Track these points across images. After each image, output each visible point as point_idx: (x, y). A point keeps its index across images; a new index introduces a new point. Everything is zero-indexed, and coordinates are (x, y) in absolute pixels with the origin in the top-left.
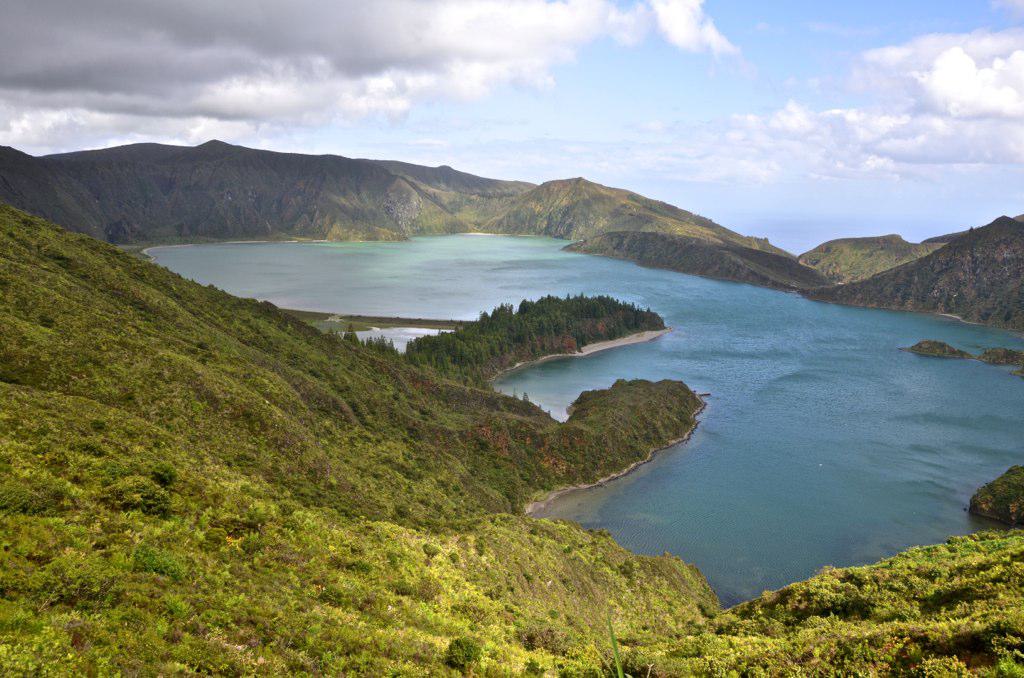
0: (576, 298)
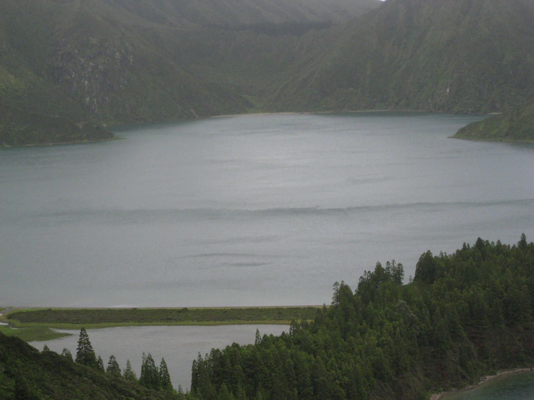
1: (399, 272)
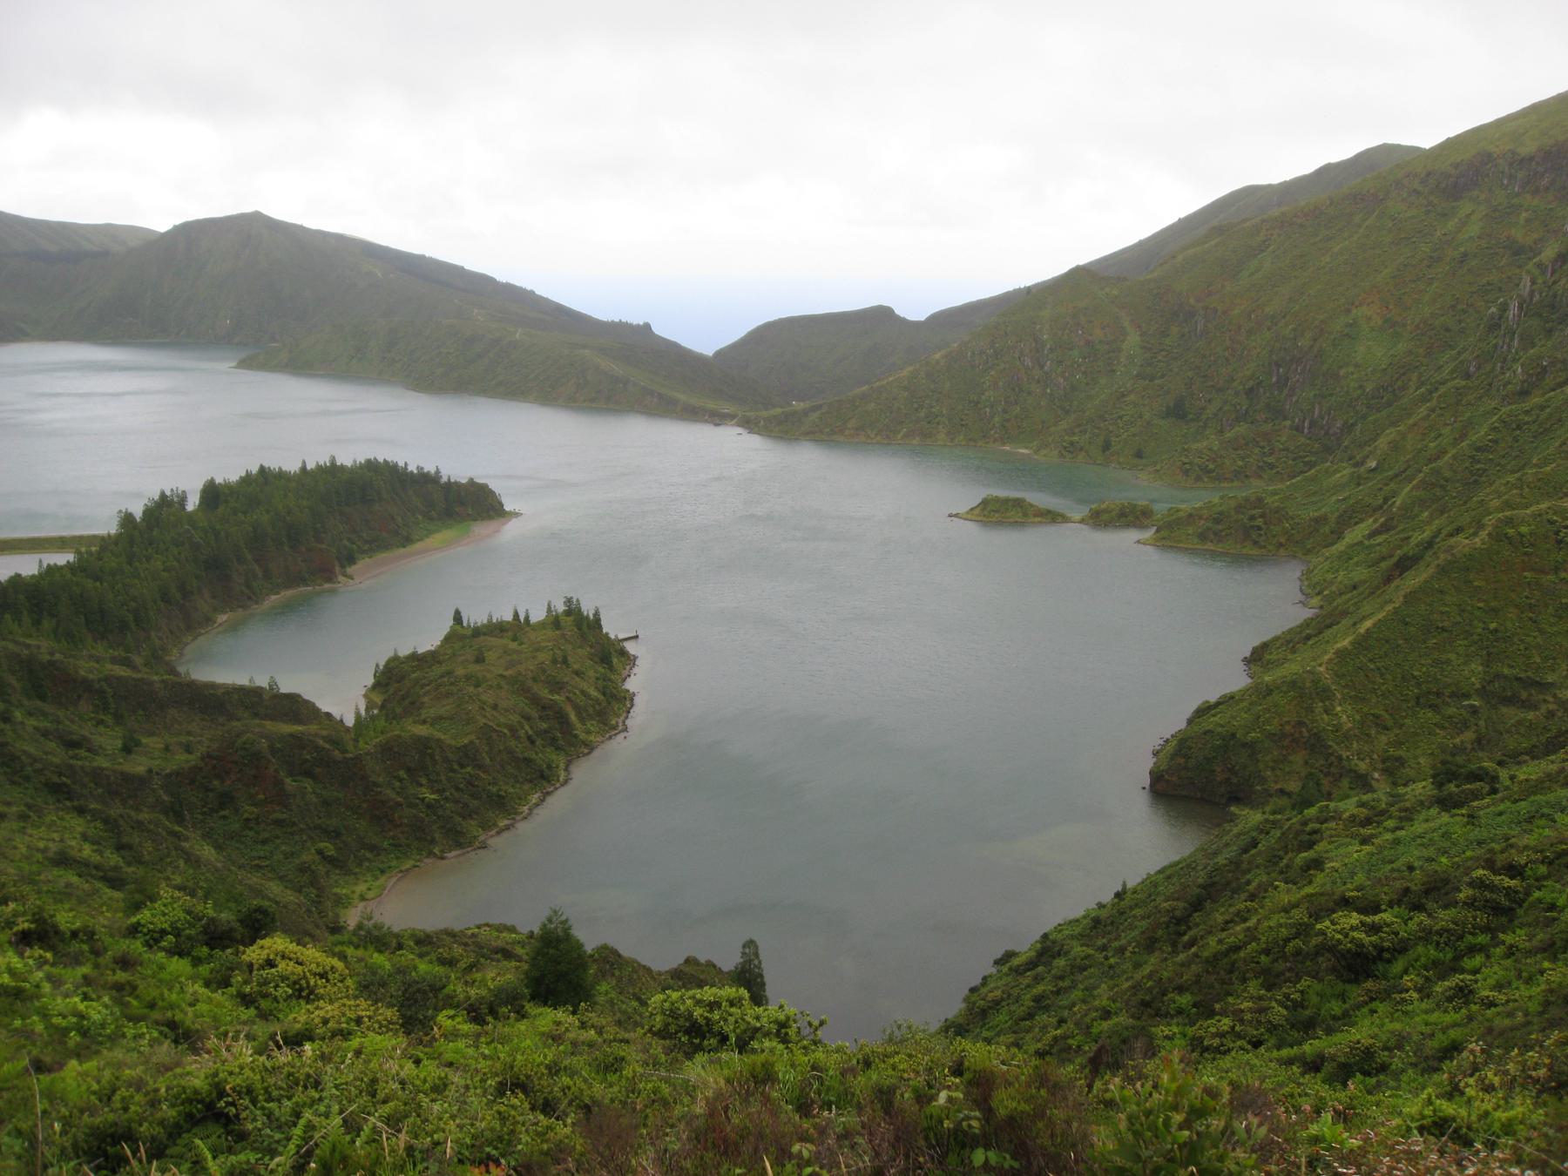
0: (319, 468)
1: (183, 499)
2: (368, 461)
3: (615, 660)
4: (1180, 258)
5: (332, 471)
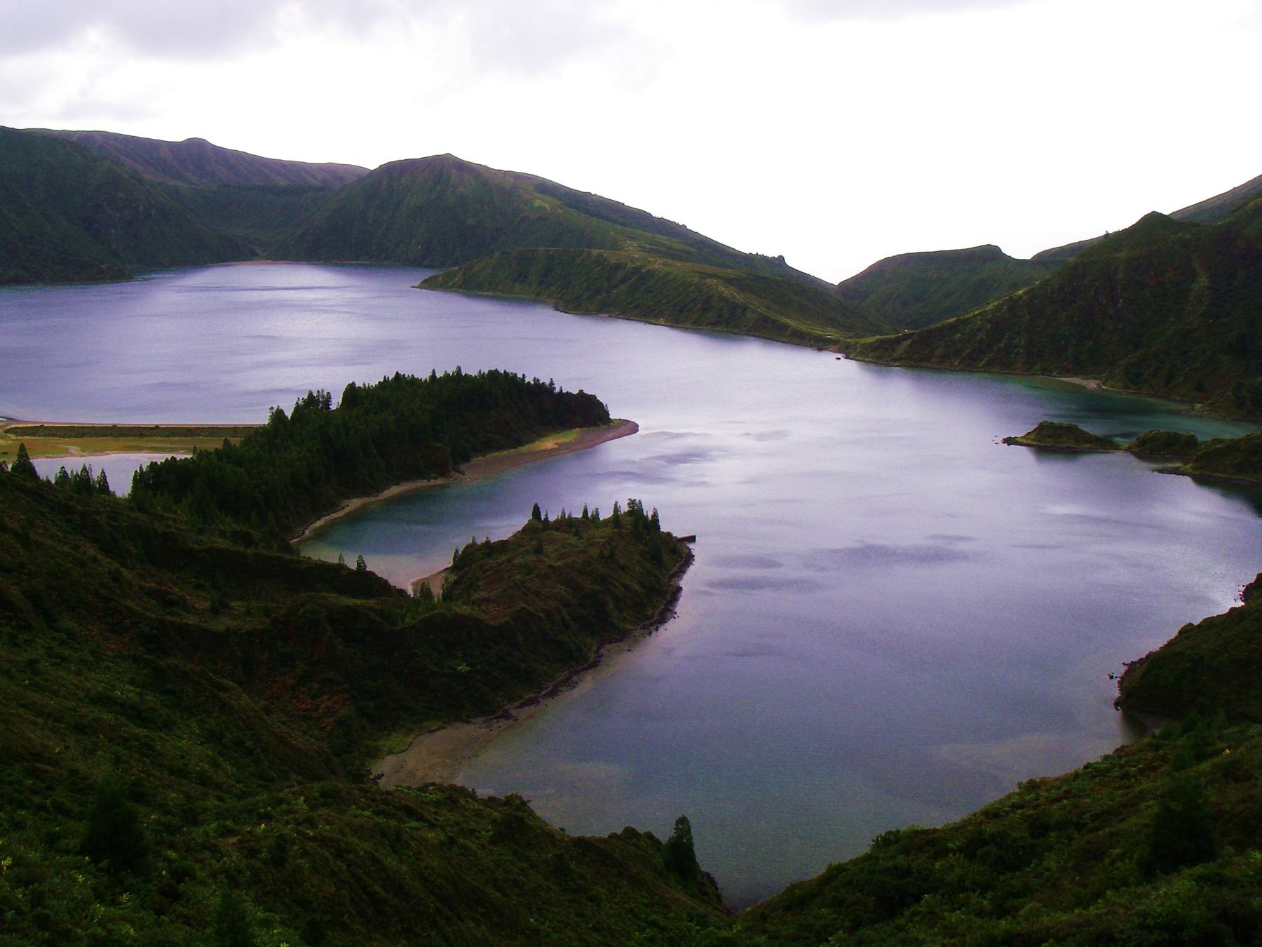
0: (447, 376)
1: (328, 399)
2: (490, 372)
3: (666, 557)
4: (1251, 204)
5: (457, 379)
